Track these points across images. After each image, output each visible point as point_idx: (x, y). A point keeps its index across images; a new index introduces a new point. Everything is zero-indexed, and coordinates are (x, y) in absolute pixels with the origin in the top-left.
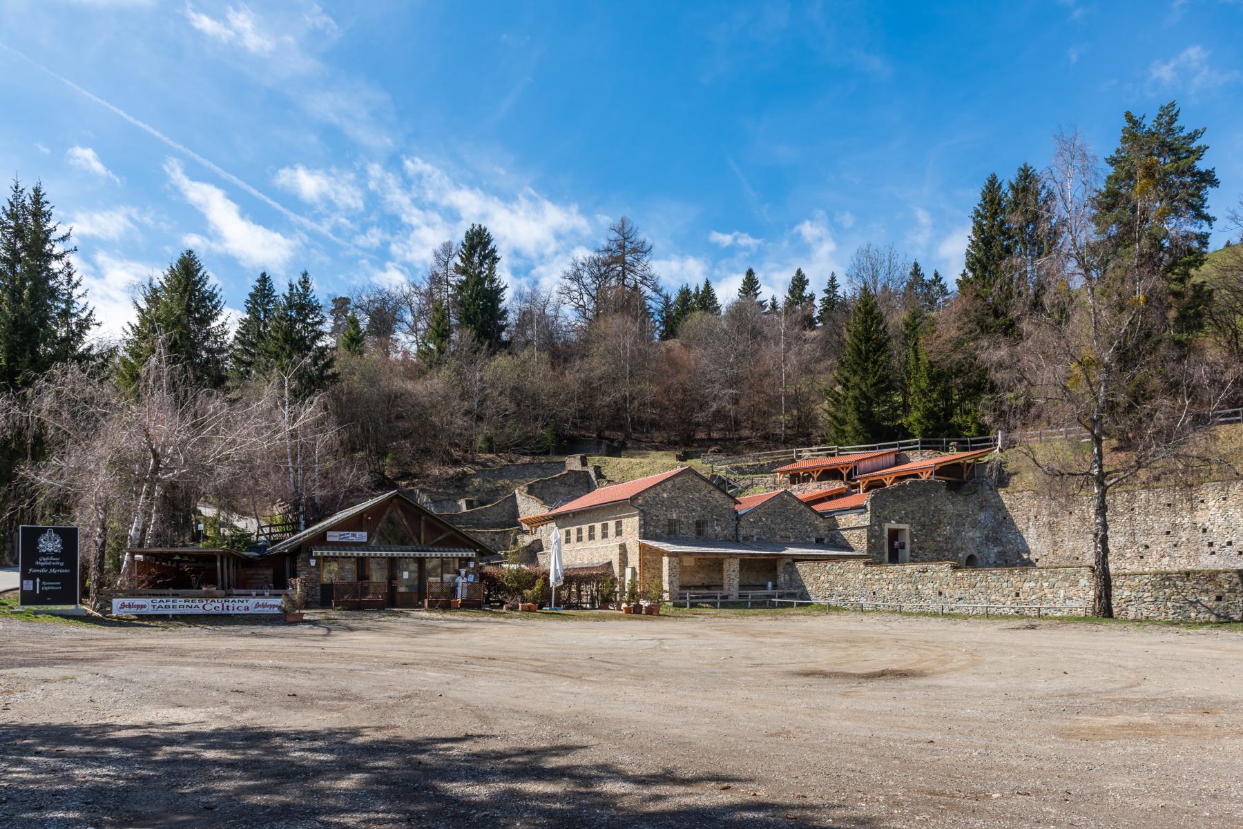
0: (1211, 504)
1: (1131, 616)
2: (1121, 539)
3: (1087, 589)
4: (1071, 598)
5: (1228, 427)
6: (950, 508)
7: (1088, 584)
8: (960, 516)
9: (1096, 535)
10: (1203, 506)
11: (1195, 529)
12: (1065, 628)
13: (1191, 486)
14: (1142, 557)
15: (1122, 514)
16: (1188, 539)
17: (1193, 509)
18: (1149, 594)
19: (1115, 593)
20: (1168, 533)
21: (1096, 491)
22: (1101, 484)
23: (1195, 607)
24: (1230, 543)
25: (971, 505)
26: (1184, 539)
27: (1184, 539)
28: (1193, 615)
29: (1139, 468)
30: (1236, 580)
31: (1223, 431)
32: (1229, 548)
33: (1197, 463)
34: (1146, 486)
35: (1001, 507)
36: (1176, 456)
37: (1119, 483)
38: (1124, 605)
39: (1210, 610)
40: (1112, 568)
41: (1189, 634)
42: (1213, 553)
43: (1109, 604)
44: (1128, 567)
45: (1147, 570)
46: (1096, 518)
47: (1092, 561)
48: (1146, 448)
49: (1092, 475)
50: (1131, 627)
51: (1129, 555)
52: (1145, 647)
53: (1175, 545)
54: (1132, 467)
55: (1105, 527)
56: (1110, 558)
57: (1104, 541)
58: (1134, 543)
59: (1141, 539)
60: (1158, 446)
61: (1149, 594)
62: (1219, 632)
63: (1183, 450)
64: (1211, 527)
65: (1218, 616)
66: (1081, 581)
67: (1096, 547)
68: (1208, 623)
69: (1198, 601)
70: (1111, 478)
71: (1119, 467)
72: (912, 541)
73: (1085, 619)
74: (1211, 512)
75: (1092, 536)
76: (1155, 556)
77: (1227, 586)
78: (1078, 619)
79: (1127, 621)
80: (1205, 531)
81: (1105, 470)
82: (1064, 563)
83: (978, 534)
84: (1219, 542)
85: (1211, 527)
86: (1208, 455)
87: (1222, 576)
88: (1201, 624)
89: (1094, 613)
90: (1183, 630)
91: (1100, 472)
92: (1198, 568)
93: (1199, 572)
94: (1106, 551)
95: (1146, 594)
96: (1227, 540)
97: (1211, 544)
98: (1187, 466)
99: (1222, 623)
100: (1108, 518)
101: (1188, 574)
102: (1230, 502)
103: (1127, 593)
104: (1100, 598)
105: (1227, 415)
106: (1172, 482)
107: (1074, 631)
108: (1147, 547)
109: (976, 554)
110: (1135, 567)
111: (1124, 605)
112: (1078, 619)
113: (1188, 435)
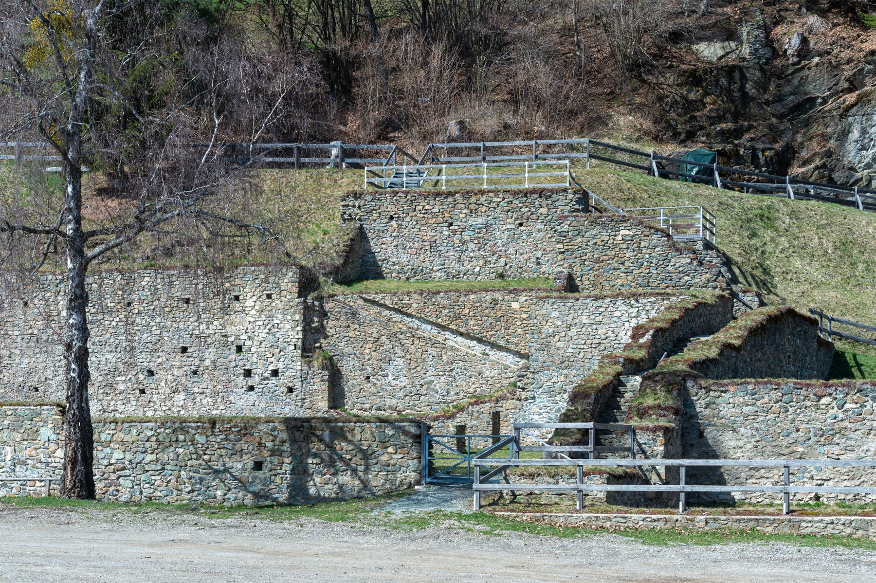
0: (249, 303)
1: (124, 497)
2: (110, 356)
3: (53, 447)
4: (24, 463)
5: (276, 173)
7: (53, 437)
9: (69, 347)
10: (237, 306)
11: (226, 345)
12: (13, 519)
13: (221, 269)
15: (110, 312)
16: (214, 362)
17: (225, 310)
18: (153, 457)
19: (98, 453)
20: (184, 350)
21: (70, 265)
22: (78, 253)
23: (222, 481)
24: (275, 373)
26: (208, 362)
27: (208, 362)
28: (219, 493)
29: (141, 230)
30: (284, 435)
31: (269, 179)
32: (274, 380)
33: (229, 229)
34: (152, 264)
36: (199, 215)
37: (105, 256)
38: (113, 477)
39: (243, 485)
40: (94, 408)
41: (213, 527)
42: (251, 388)
43: (89, 474)
44: (121, 408)
45: (150, 414)
46: (70, 316)
47: (61, 395)
48: (154, 194)
49: (64, 235)
50: (125, 515)
51: (121, 387)
52: (146, 551)
53: (195, 373)
54: (130, 227)
55: (84, 332)
56: (91, 391)
57: (82, 357)
58: (130, 365)
59: (144, 360)
60: (171, 193)
61: (153, 457)
62: (258, 522)
63: (210, 205)
64: (249, 343)
65: (256, 495)
66: (43, 430)
67: (68, 369)
68: (240, 507)
69: (227, 470)
70: (96, 245)
71: (108, 225)
73: (48, 501)
74: (249, 319)
75: (61, 349)
76: (164, 389)
77: (269, 445)
78: (36, 502)
79: (116, 504)
80: (239, 349)
81: (86, 228)
82: (12, 396)
84: (259, 370)
85: (249, 343)
86: (248, 220)
87: (261, 427)
88: (231, 509)
89: (63, 491)
90: (205, 520)
91: (77, 230)
92: (228, 414)
93: (230, 421)
94: (84, 376)
95: (149, 458)
96: (271, 368)
97: (248, 373)
98: (215, 234)
99: (261, 507)
100: (89, 317)
101: (213, 422)
102: (276, 303)
103: (118, 455)
104: (74, 462)
105: (276, 153)
106: (192, 260)
107: (30, 524)
108: (151, 373)
110: (132, 409)
111: (113, 477)
112: (36, 502)
113: (216, 179)
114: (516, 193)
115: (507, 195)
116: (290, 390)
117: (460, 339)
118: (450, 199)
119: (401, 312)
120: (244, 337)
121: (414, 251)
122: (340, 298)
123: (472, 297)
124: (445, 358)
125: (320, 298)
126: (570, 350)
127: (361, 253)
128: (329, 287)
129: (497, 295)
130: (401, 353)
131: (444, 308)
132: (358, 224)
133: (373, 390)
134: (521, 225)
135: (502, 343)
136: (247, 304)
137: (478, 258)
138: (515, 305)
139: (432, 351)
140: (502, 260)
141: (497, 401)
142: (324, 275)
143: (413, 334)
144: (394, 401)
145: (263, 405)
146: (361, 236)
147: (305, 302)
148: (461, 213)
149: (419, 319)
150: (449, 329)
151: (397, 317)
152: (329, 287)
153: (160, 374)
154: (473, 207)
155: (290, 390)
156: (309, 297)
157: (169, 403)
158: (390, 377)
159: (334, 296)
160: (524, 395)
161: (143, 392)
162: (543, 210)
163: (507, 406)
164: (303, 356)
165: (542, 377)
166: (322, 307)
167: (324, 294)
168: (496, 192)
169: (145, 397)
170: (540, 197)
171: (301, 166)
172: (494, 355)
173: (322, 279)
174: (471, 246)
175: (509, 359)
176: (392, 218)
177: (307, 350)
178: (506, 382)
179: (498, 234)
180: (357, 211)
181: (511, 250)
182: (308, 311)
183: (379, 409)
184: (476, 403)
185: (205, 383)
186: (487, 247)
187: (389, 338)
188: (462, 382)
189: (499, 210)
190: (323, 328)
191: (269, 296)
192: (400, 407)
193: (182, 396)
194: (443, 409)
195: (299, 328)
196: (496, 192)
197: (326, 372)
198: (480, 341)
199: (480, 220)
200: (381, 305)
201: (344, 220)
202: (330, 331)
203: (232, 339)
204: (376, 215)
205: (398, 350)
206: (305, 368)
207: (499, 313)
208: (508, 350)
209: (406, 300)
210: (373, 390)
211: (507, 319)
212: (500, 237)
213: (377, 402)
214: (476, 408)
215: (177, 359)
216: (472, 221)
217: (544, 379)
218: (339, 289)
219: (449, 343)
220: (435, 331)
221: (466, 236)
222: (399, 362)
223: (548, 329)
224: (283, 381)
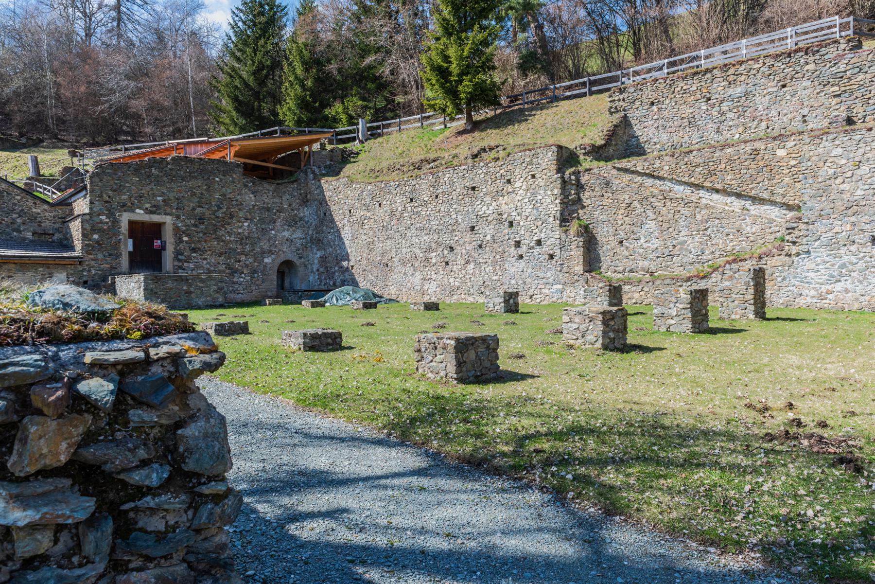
0: (518, 184)
2: (426, 238)
6: (249, 198)
8: (268, 210)
10: (509, 188)
14: (447, 263)
16: (493, 237)
24: (539, 243)
25: (286, 197)
27: (489, 237)
32: (538, 249)
35: (322, 202)
42: (521, 257)
53: (480, 246)
64: (518, 218)
72: (179, 240)
80: (511, 224)
83: (298, 234)
84: (528, 240)
96: (535, 238)
97: (518, 244)
102: (539, 181)
109: (295, 259)
114: (777, 57)
115: (767, 60)
116: (551, 257)
117: (715, 196)
118: (708, 75)
119: (653, 177)
120: (514, 214)
121: (673, 129)
122: (596, 171)
123: (729, 150)
124: (699, 217)
125: (577, 174)
126: (860, 192)
127: (625, 138)
128: (587, 162)
129: (759, 145)
130: (652, 216)
131: (697, 166)
132: (622, 114)
133: (626, 253)
134: (784, 86)
135: (765, 195)
136: (516, 185)
137: (737, 126)
138: (781, 153)
139: (685, 211)
140: (764, 125)
141: (760, 258)
142: (584, 154)
143: (665, 197)
144: (646, 263)
145: (530, 270)
146: (625, 122)
147: (562, 178)
148: (718, 87)
149: (671, 180)
150: (703, 187)
151: (650, 181)
152: (587, 162)
153: (458, 249)
154: (731, 78)
155: (551, 257)
156: (567, 173)
157: (464, 272)
158: (642, 240)
159: (590, 170)
160: (794, 250)
161: (447, 263)
162: (811, 67)
163: (769, 264)
164: (561, 226)
165: (820, 227)
166: (578, 180)
167: (580, 168)
168: (756, 60)
169: (448, 268)
170: (807, 54)
171: (592, 93)
172: (755, 209)
173: (582, 157)
174: (730, 115)
175: (774, 213)
176: (652, 104)
177: (564, 220)
178: (770, 238)
179: (758, 99)
180: (621, 103)
181: (774, 113)
182: (564, 182)
183: (631, 271)
184: (734, 261)
185: (486, 255)
186: (747, 114)
187: (641, 202)
188: (718, 240)
189: (759, 76)
190: (579, 200)
191: (533, 176)
192: (653, 268)
193: (472, 266)
194: (697, 269)
195: (558, 201)
196: (756, 60)
197: (581, 239)
198: (739, 196)
199: (739, 90)
200: (633, 172)
201: (611, 113)
202: (586, 202)
203: (505, 216)
204: (638, 103)
205: (650, 213)
206: (563, 236)
207: (761, 164)
208: (773, 203)
209: (657, 164)
210: (626, 253)
211: (771, 169)
212: (761, 102)
213: (630, 264)
214: (735, 266)
215: (468, 237)
216: (730, 91)
217: (822, 229)
218: (595, 164)
219: (704, 201)
220: (688, 191)
221: (725, 107)
222: (651, 225)
223: (827, 171)
224: (546, 249)
